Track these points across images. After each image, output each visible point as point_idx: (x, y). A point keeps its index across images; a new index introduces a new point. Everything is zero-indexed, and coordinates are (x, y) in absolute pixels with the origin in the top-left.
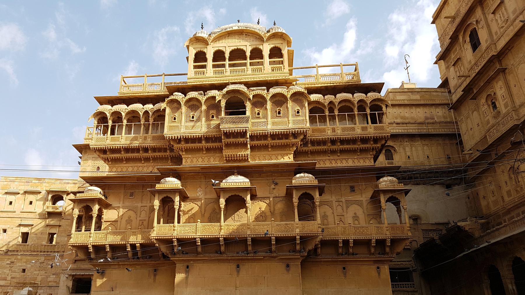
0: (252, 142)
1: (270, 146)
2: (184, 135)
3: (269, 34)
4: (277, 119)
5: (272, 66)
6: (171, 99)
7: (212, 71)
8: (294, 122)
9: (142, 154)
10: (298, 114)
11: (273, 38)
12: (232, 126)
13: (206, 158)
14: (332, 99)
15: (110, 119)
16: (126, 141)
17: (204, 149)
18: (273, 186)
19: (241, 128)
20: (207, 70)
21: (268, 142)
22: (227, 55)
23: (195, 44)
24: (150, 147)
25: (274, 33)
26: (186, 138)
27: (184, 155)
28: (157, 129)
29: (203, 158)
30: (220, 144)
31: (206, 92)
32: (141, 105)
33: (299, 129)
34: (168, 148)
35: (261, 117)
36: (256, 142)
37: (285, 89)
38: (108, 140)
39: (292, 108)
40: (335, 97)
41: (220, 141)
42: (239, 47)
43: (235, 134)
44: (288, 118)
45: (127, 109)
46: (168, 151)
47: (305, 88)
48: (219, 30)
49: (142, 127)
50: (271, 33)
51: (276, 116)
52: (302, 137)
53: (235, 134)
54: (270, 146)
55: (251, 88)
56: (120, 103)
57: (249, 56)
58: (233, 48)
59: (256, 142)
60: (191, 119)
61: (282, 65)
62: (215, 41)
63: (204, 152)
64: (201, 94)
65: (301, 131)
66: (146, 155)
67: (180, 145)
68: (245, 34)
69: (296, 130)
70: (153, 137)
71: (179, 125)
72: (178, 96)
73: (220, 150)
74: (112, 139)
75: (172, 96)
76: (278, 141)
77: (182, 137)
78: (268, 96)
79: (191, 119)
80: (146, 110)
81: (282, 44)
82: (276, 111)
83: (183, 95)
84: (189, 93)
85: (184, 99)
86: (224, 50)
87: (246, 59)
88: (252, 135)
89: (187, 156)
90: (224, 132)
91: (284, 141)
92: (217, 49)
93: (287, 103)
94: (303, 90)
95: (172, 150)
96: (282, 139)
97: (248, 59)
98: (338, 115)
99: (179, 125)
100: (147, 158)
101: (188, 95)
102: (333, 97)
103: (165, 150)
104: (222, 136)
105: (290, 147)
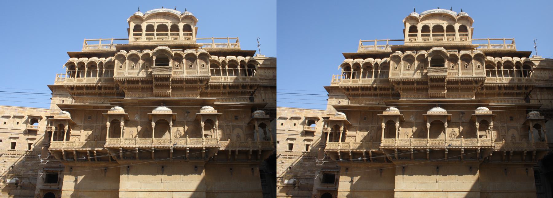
0: (448, 86)
1: (460, 89)
2: (402, 79)
3: (458, 17)
4: (466, 71)
5: (461, 37)
6: (394, 55)
7: (421, 39)
8: (476, 73)
9: (372, 92)
10: (479, 68)
11: (461, 19)
12: (435, 74)
13: (417, 95)
14: (500, 60)
15: (352, 68)
16: (362, 82)
17: (415, 89)
18: (461, 115)
19: (442, 75)
20: (417, 38)
21: (459, 86)
22: (431, 29)
23: (410, 21)
24: (378, 87)
25: (462, 16)
26: (403, 81)
27: (401, 92)
28: (383, 75)
29: (415, 95)
30: (427, 86)
31: (418, 51)
32: (373, 59)
33: (480, 78)
34: (390, 88)
35: (455, 69)
36: (450, 86)
37: (470, 52)
38: (350, 82)
39: (475, 65)
40: (501, 59)
41: (427, 84)
42: (439, 24)
43: (437, 79)
44: (472, 70)
45: (364, 62)
46: (390, 90)
47: (483, 52)
48: (426, 13)
49: (373, 74)
50: (460, 16)
51: (465, 69)
52: (481, 84)
53: (437, 79)
54: (460, 89)
55: (448, 50)
56: (359, 58)
57: (445, 30)
58: (435, 24)
59: (450, 86)
60: (407, 69)
61: (467, 37)
62: (423, 19)
63: (416, 91)
64: (414, 52)
65: (480, 79)
66: (375, 92)
67: (399, 86)
68: (443, 16)
69: (478, 78)
70: (381, 80)
71: (399, 72)
72: (399, 53)
73: (427, 90)
74: (353, 81)
75: (394, 53)
76: (465, 85)
77: (401, 80)
78: (459, 55)
79: (407, 69)
80: (376, 62)
81: (467, 23)
82: (465, 66)
83: (402, 53)
84: (406, 52)
85: (403, 55)
86: (429, 25)
87: (443, 31)
88: (448, 81)
89: (404, 93)
90: (430, 78)
91: (469, 86)
92: (425, 24)
93: (472, 61)
94: (482, 53)
95: (393, 89)
96: (467, 84)
97: (445, 32)
98: (503, 70)
99: (399, 72)
100: (376, 94)
101: (406, 53)
102: (500, 58)
103: (388, 89)
104: (429, 81)
105: (473, 90)
